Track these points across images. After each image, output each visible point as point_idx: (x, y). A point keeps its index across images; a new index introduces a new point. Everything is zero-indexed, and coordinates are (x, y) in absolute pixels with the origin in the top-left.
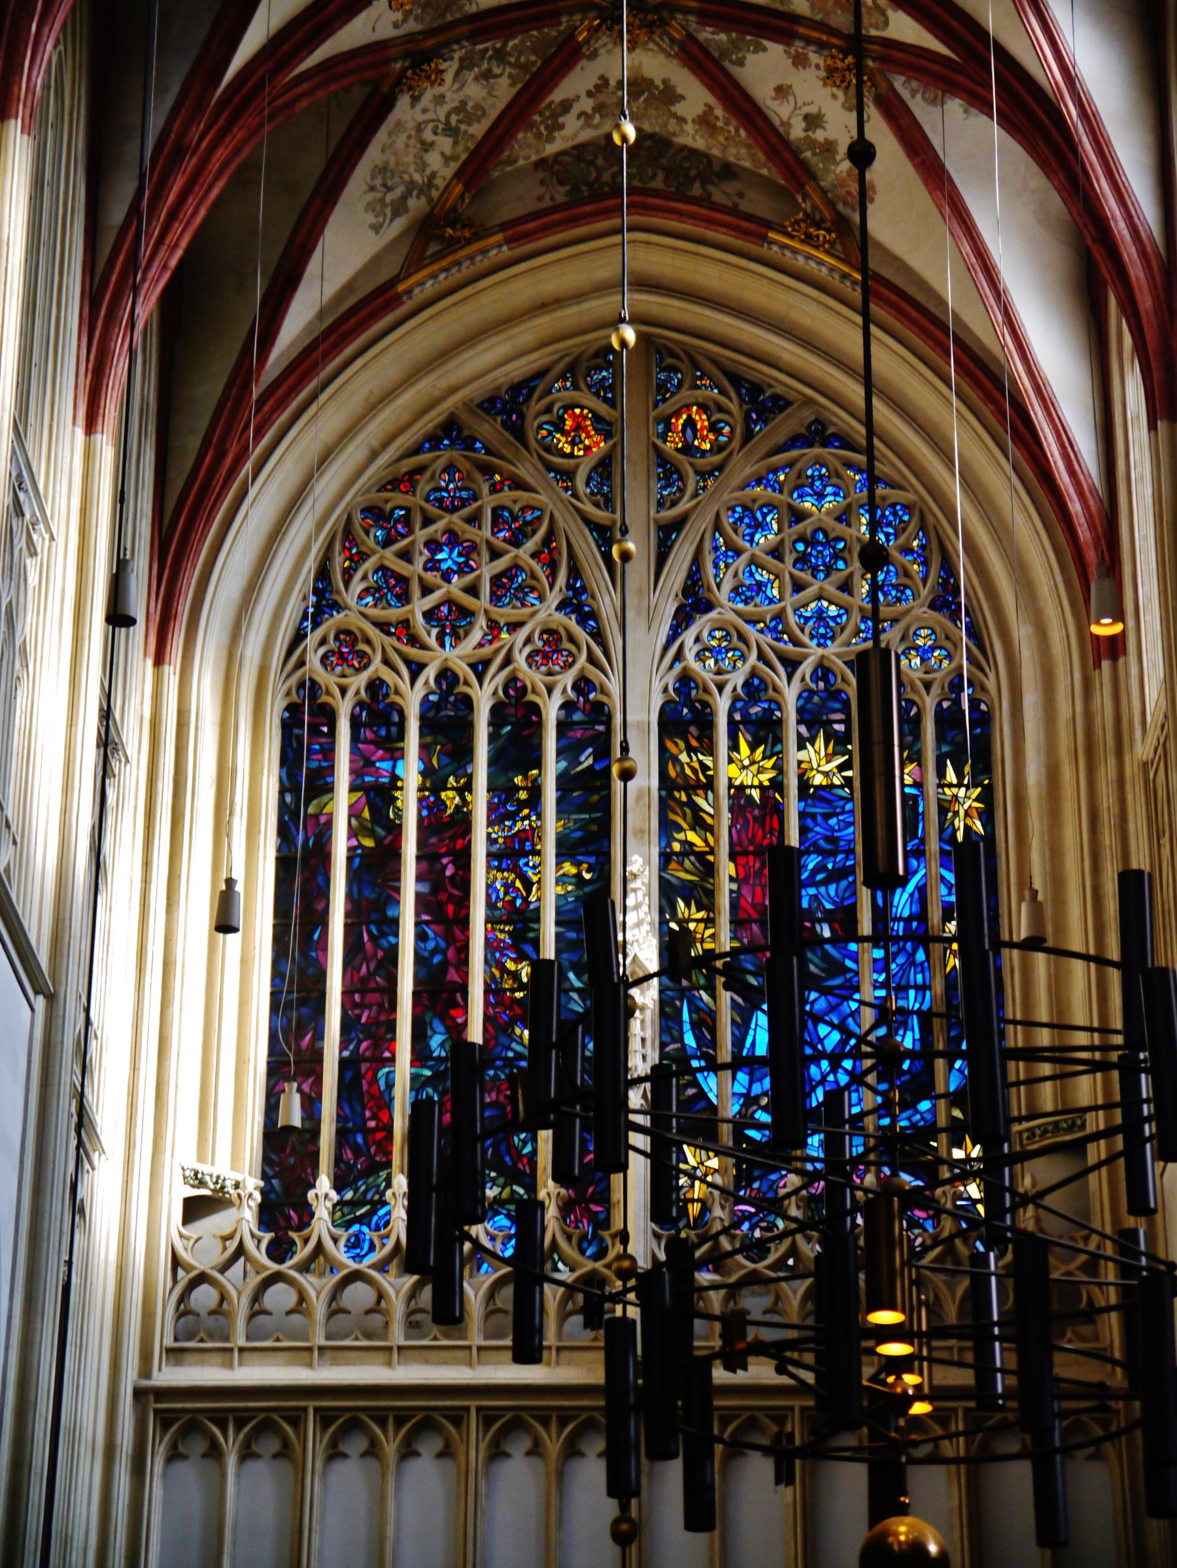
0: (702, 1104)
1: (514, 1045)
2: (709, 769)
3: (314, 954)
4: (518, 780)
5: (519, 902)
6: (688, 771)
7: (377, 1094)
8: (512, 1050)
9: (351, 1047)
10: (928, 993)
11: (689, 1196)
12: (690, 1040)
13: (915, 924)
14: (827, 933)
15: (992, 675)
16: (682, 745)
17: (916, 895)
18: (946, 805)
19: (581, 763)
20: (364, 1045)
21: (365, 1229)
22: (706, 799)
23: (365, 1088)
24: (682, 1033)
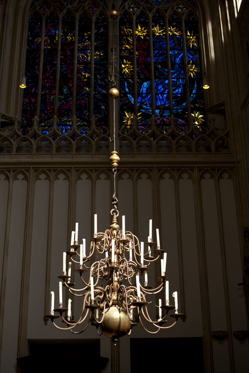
0: (130, 104)
1: (84, 91)
2: (131, 32)
3: (35, 71)
4: (85, 34)
5: (85, 60)
6: (126, 32)
7: (50, 102)
8: (84, 92)
9: (44, 91)
10: (184, 80)
11: (127, 124)
12: (127, 90)
13: (181, 65)
14: (160, 67)
15: (198, 12)
16: (125, 27)
17: (181, 59)
18: (188, 40)
19: (101, 31)
20: (47, 91)
21: (47, 132)
22: (131, 38)
23: (47, 100)
24: (125, 88)
